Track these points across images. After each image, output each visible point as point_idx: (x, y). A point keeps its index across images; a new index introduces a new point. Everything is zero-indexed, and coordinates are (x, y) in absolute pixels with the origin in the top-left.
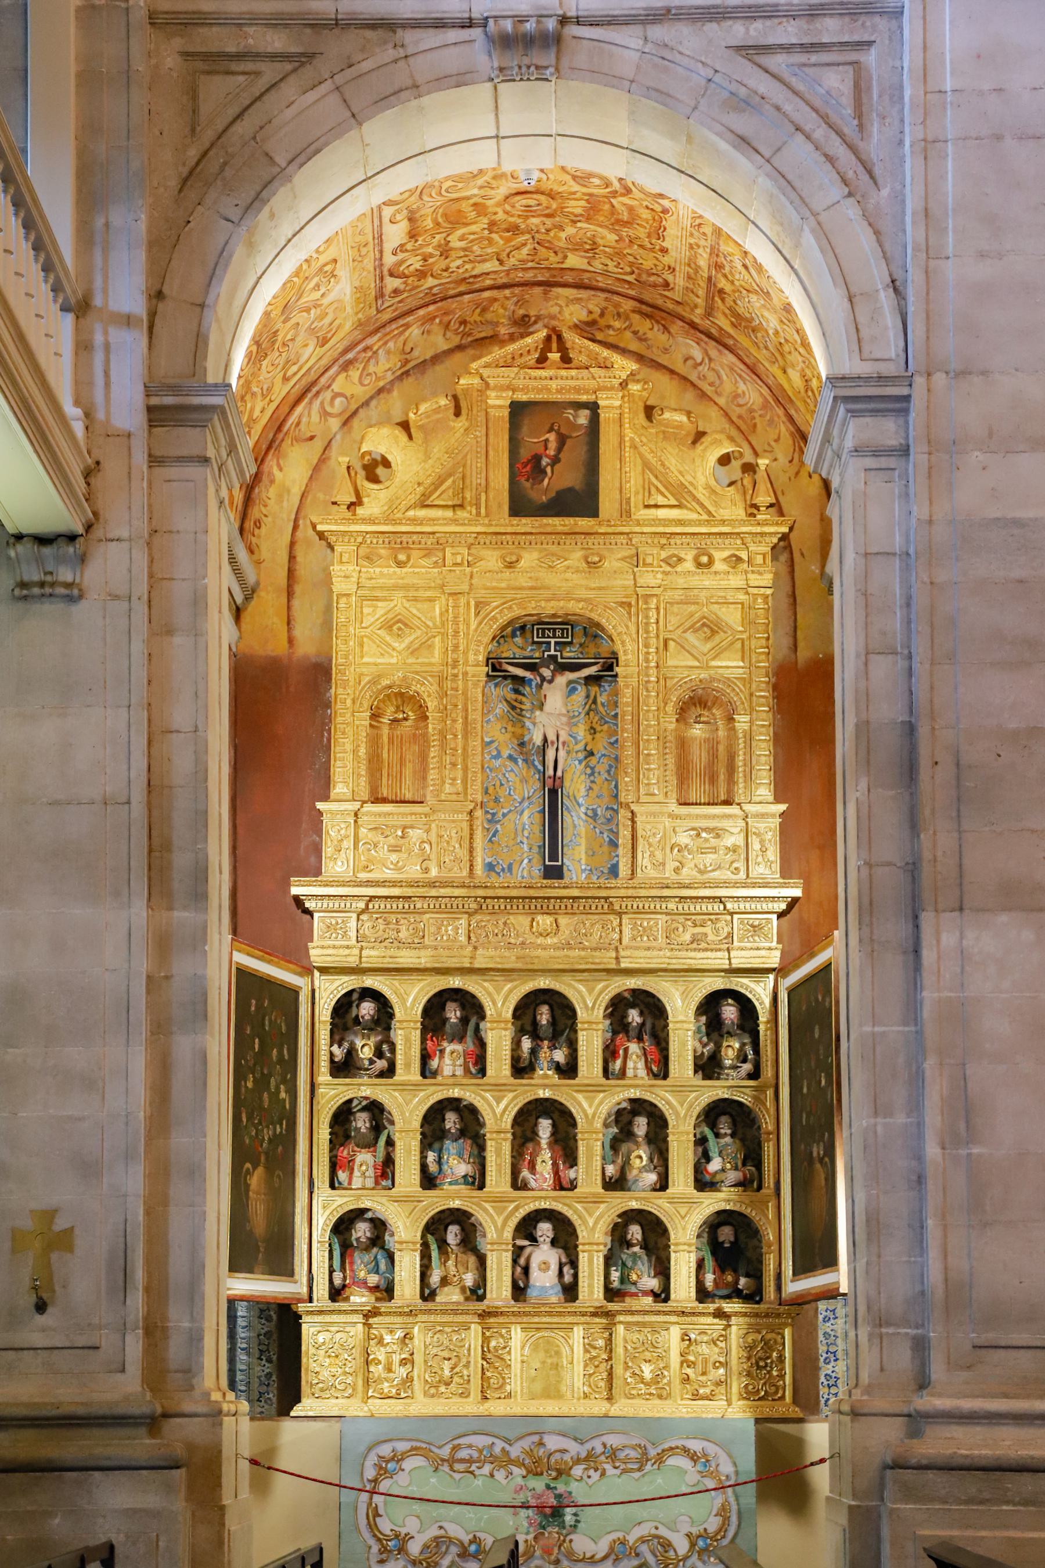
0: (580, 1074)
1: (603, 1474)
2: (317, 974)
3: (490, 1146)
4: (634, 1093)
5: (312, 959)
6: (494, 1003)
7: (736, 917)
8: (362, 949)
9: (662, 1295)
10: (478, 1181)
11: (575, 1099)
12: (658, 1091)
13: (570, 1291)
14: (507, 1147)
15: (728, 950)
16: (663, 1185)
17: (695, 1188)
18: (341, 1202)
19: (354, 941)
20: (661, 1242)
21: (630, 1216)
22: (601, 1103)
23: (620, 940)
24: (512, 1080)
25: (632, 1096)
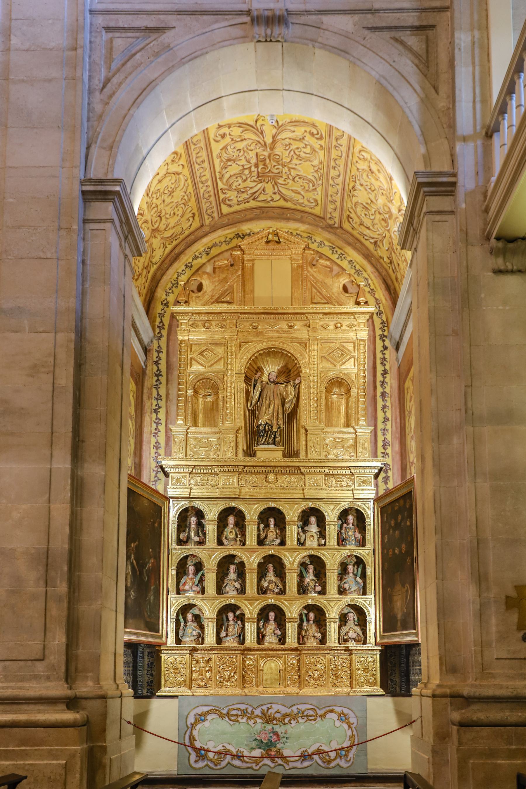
0: (287, 544)
1: (298, 721)
2: (171, 500)
3: (248, 576)
4: (311, 552)
5: (169, 493)
6: (250, 514)
7: (356, 476)
8: (191, 489)
9: (323, 641)
10: (242, 591)
11: (285, 555)
12: (320, 551)
13: (282, 639)
14: (255, 576)
15: (352, 490)
16: (323, 592)
17: (338, 594)
18: (182, 600)
19: (187, 486)
20: (322, 618)
21: (309, 608)
22: (297, 556)
23: (305, 485)
24: (257, 547)
25: (310, 554)
